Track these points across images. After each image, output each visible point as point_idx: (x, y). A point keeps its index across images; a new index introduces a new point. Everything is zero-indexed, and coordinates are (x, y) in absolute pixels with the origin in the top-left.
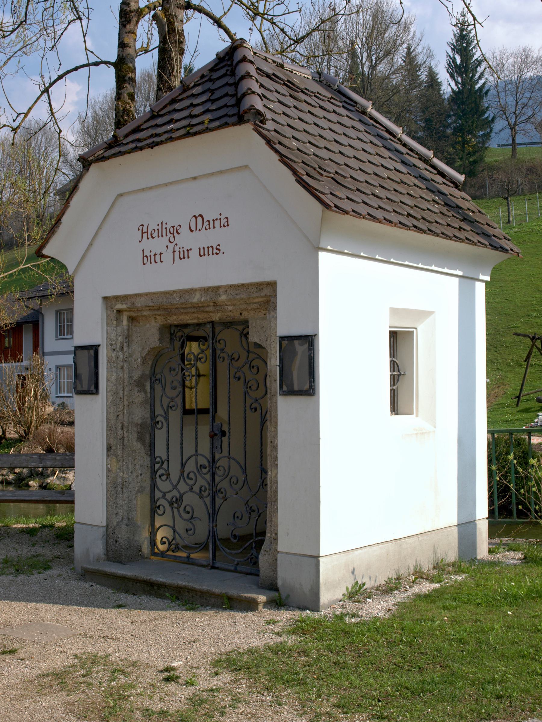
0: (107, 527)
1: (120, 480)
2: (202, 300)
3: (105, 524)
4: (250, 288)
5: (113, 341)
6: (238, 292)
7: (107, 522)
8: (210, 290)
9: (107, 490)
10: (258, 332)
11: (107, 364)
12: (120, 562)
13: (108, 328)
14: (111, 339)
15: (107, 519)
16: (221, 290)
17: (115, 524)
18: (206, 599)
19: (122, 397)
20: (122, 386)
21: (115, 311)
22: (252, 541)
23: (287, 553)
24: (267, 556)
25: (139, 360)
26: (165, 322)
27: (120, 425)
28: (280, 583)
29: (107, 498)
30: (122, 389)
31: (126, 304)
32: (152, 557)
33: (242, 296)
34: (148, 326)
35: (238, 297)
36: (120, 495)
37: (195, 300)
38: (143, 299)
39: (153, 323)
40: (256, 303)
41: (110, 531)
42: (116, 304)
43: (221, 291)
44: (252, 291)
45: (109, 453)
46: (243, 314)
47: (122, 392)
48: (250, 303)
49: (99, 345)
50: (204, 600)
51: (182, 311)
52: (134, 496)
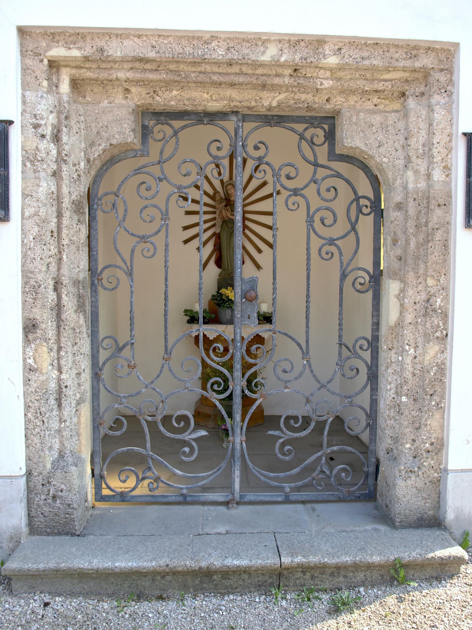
0: (29, 474)
1: (53, 385)
2: (283, 59)
3: (24, 471)
4: (392, 50)
5: (42, 119)
6: (366, 54)
7: (27, 466)
8: (302, 44)
9: (27, 407)
10: (363, 131)
11: (24, 165)
12: (67, 534)
13: (28, 93)
14: (35, 116)
15: (29, 459)
16: (326, 47)
17: (49, 466)
18: (345, 577)
19: (55, 230)
20: (54, 209)
21: (46, 62)
22: (319, 454)
23: (462, 471)
24: (413, 478)
25: (82, 164)
26: (150, 101)
27: (52, 283)
28: (450, 516)
29: (28, 421)
30: (55, 214)
31: (80, 49)
32: (98, 504)
33: (376, 62)
34: (105, 103)
35: (367, 62)
36: (55, 413)
37: (266, 58)
38: (128, 43)
39: (119, 99)
40: (386, 81)
41: (38, 480)
42: (49, 48)
43: (327, 49)
44: (397, 56)
45: (31, 337)
46: (333, 101)
47: (55, 220)
48: (373, 80)
49: (11, 122)
50: (341, 579)
51: (215, 78)
52: (75, 410)
